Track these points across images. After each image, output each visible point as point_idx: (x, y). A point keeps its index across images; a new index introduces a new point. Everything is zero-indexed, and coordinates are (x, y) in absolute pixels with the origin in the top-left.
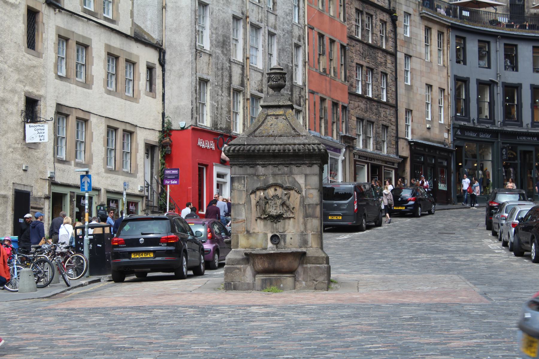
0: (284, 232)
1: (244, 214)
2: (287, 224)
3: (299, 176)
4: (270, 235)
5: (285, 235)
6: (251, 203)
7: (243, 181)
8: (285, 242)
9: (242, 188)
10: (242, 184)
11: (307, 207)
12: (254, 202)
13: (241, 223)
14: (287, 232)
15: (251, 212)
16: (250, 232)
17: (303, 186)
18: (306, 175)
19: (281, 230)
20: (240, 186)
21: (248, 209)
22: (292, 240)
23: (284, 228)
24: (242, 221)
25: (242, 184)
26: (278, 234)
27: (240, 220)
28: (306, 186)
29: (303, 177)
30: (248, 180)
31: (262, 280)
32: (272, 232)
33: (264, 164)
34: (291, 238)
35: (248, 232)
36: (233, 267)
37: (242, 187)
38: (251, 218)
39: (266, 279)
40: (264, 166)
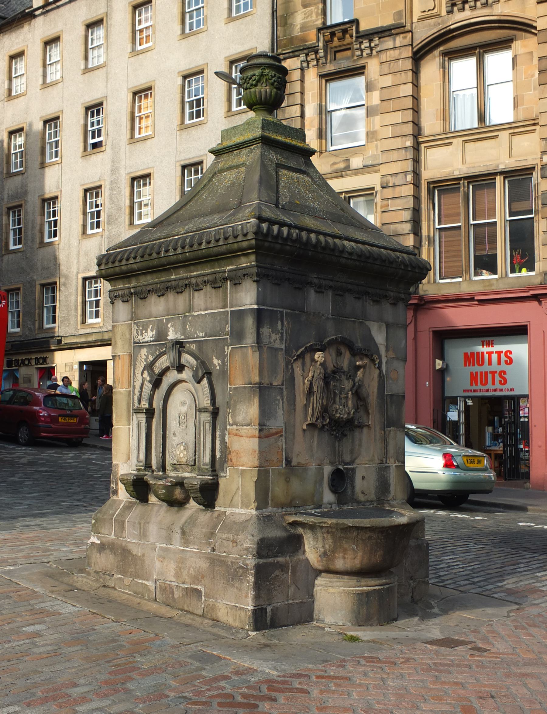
0: (352, 462)
1: (280, 412)
2: (357, 442)
3: (375, 323)
4: (328, 470)
5: (354, 470)
6: (294, 385)
7: (280, 322)
8: (353, 487)
9: (277, 345)
10: (279, 332)
11: (389, 401)
12: (301, 386)
13: (275, 437)
14: (357, 461)
15: (295, 409)
16: (293, 464)
17: (382, 350)
18: (388, 326)
19: (347, 458)
20: (274, 336)
21: (288, 402)
22: (365, 481)
23: (352, 452)
24: (277, 433)
25: (279, 332)
26: (340, 467)
27: (274, 431)
28: (387, 350)
29: (384, 328)
30: (288, 324)
31: (360, 595)
32: (332, 463)
33: (320, 286)
34: (363, 478)
35: (288, 461)
36: (271, 564)
37: (278, 341)
38: (294, 426)
39: (368, 594)
40: (320, 290)
